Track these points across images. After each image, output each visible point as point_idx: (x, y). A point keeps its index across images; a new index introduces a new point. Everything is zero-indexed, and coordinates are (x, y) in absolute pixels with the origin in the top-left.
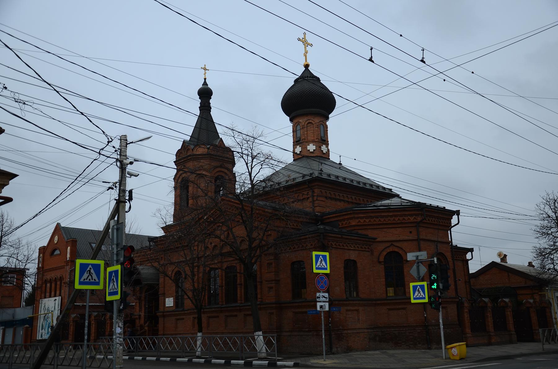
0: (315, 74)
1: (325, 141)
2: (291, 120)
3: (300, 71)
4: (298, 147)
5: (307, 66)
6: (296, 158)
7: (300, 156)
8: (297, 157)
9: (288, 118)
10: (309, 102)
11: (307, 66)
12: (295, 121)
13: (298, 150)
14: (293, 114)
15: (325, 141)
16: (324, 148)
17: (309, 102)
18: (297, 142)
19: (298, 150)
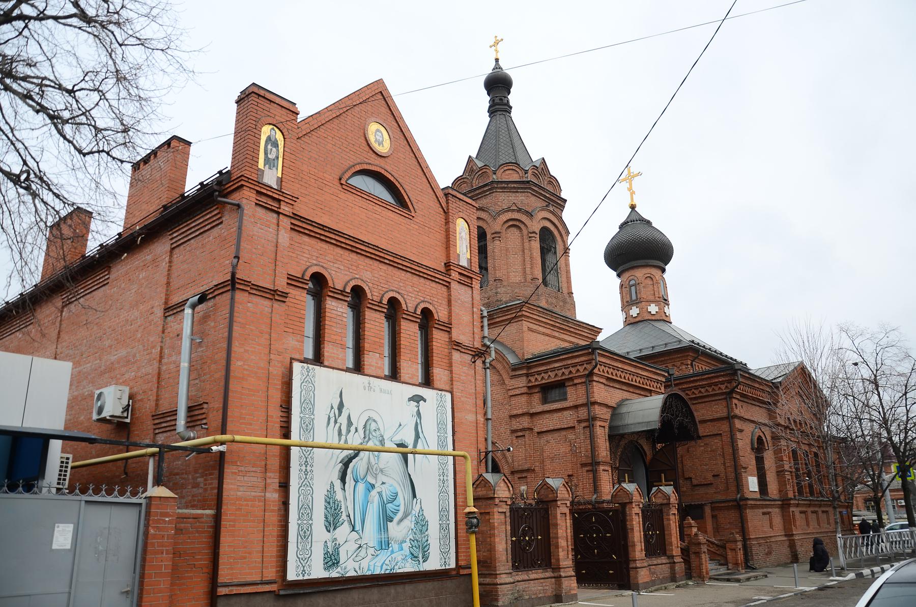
0: (646, 216)
1: (666, 301)
2: (619, 276)
3: (623, 214)
4: (634, 308)
5: (633, 207)
6: (633, 321)
7: (637, 320)
8: (630, 322)
9: (614, 273)
11: (633, 207)
12: (626, 275)
13: (634, 311)
14: (621, 268)
16: (666, 309)
17: (639, 253)
18: (627, 304)
19: (634, 311)
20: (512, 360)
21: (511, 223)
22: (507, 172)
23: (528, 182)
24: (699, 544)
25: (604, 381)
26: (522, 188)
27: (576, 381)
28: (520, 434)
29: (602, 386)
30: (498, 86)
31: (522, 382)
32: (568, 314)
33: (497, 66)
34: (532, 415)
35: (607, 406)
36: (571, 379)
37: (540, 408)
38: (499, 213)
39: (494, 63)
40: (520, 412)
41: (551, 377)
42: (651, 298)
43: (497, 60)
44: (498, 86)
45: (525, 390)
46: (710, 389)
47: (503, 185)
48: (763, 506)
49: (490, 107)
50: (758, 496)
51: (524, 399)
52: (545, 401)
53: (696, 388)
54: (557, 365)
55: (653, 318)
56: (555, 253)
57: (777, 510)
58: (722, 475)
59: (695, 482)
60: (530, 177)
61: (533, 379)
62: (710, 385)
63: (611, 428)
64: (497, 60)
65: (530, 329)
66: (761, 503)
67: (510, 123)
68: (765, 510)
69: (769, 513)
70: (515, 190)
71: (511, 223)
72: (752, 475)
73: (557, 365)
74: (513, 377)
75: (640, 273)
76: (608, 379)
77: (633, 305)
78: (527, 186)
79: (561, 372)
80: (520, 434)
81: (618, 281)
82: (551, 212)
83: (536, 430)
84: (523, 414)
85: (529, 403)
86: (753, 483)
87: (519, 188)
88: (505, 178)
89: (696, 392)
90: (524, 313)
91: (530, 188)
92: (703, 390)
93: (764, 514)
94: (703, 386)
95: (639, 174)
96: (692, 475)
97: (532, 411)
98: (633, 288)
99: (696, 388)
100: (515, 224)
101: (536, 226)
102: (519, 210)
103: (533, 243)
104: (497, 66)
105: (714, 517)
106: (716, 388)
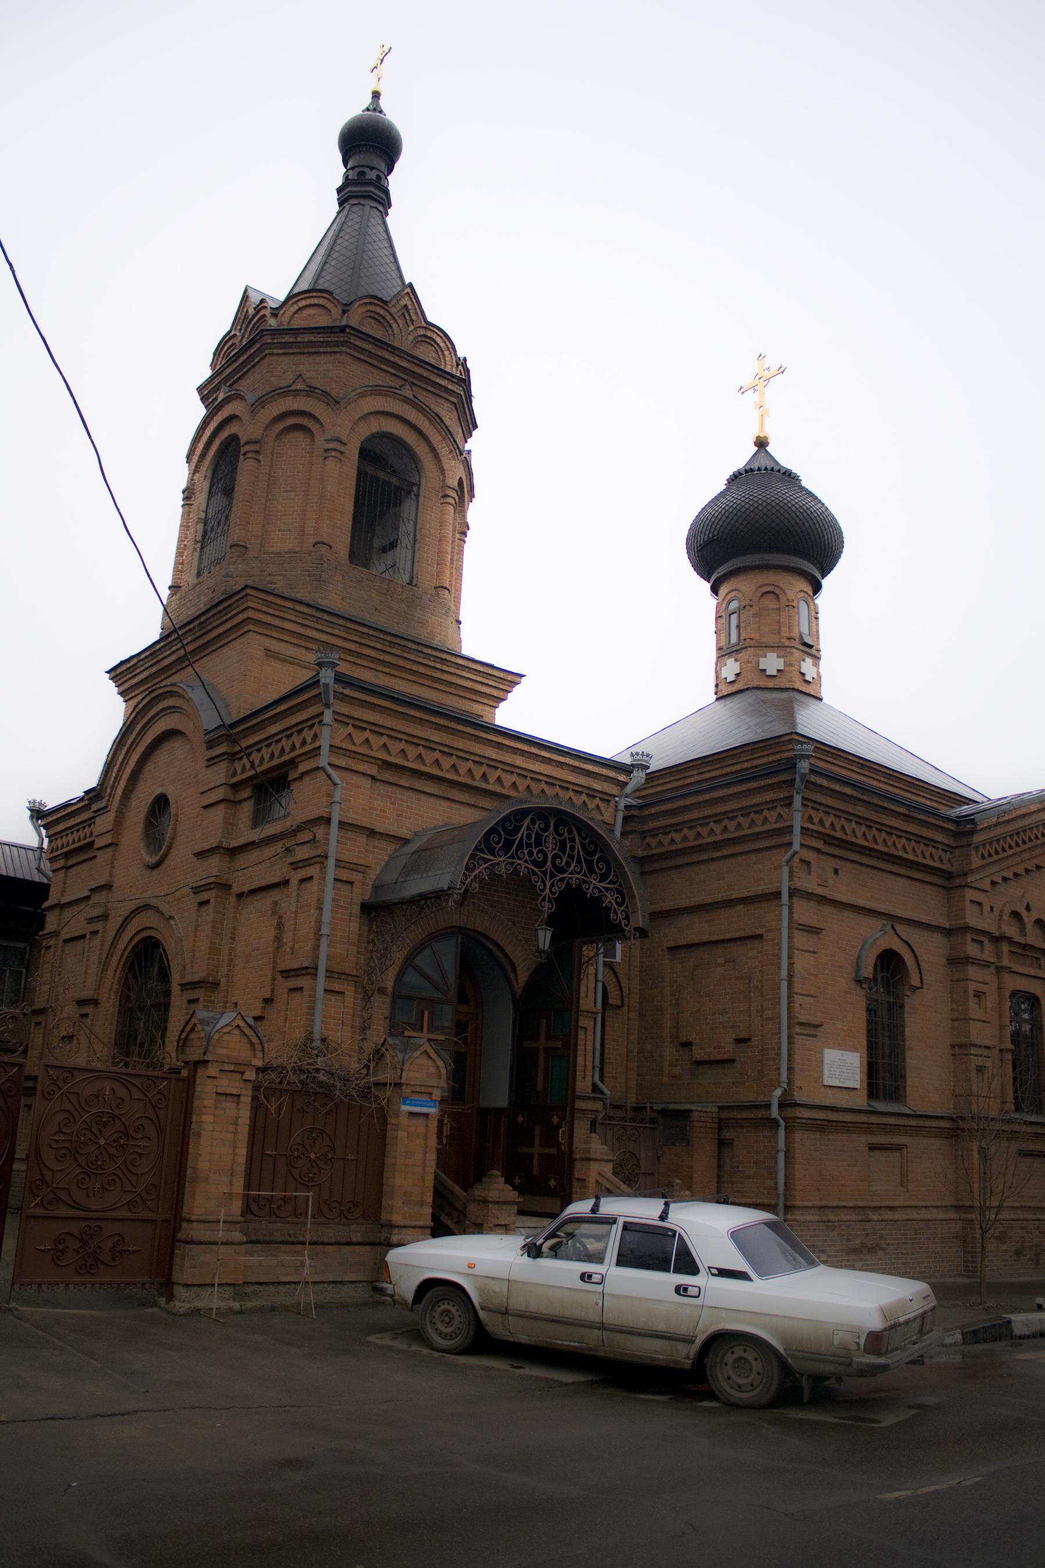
2: (715, 590)
3: (741, 456)
5: (761, 444)
9: (707, 586)
10: (764, 541)
11: (761, 444)
12: (723, 590)
15: (811, 647)
16: (807, 666)
17: (764, 541)
20: (209, 720)
21: (291, 421)
22: (306, 312)
23: (342, 329)
24: (485, 1201)
25: (373, 770)
26: (328, 344)
27: (303, 767)
28: (204, 896)
29: (367, 783)
30: (370, 148)
31: (219, 774)
32: (422, 635)
33: (375, 106)
34: (233, 852)
35: (372, 833)
36: (293, 763)
37: (246, 834)
38: (262, 402)
39: (367, 100)
40: (206, 846)
41: (265, 760)
42: (772, 639)
43: (376, 95)
44: (370, 148)
45: (220, 794)
46: (745, 822)
47: (288, 339)
48: (869, 1129)
49: (339, 190)
50: (861, 1101)
51: (219, 813)
52: (259, 818)
53: (718, 818)
54: (274, 729)
55: (770, 685)
56: (417, 496)
57: (936, 1143)
58: (755, 1040)
59: (699, 1054)
60: (353, 319)
61: (238, 766)
62: (745, 812)
63: (376, 888)
64: (376, 95)
65: (269, 653)
66: (862, 1118)
67: (375, 220)
68: (883, 1139)
69: (899, 1148)
70: (313, 350)
71: (291, 421)
72: (841, 1046)
73: (274, 729)
74: (212, 762)
75: (746, 585)
76: (387, 765)
77: (729, 654)
78: (342, 338)
79: (279, 746)
80: (204, 896)
81: (710, 603)
82: (406, 400)
83: (236, 889)
84: (212, 851)
85: (229, 825)
86: (842, 1067)
87: (320, 344)
88: (299, 322)
89: (718, 828)
90: (250, 613)
91: (346, 343)
92: (731, 825)
93: (872, 1148)
94: (730, 815)
95: (781, 370)
96: (693, 1037)
97: (234, 844)
98: (734, 617)
99: (718, 818)
100: (298, 424)
101: (349, 427)
102: (311, 391)
103: (331, 463)
104: (375, 106)
105: (721, 1144)
106: (758, 819)
